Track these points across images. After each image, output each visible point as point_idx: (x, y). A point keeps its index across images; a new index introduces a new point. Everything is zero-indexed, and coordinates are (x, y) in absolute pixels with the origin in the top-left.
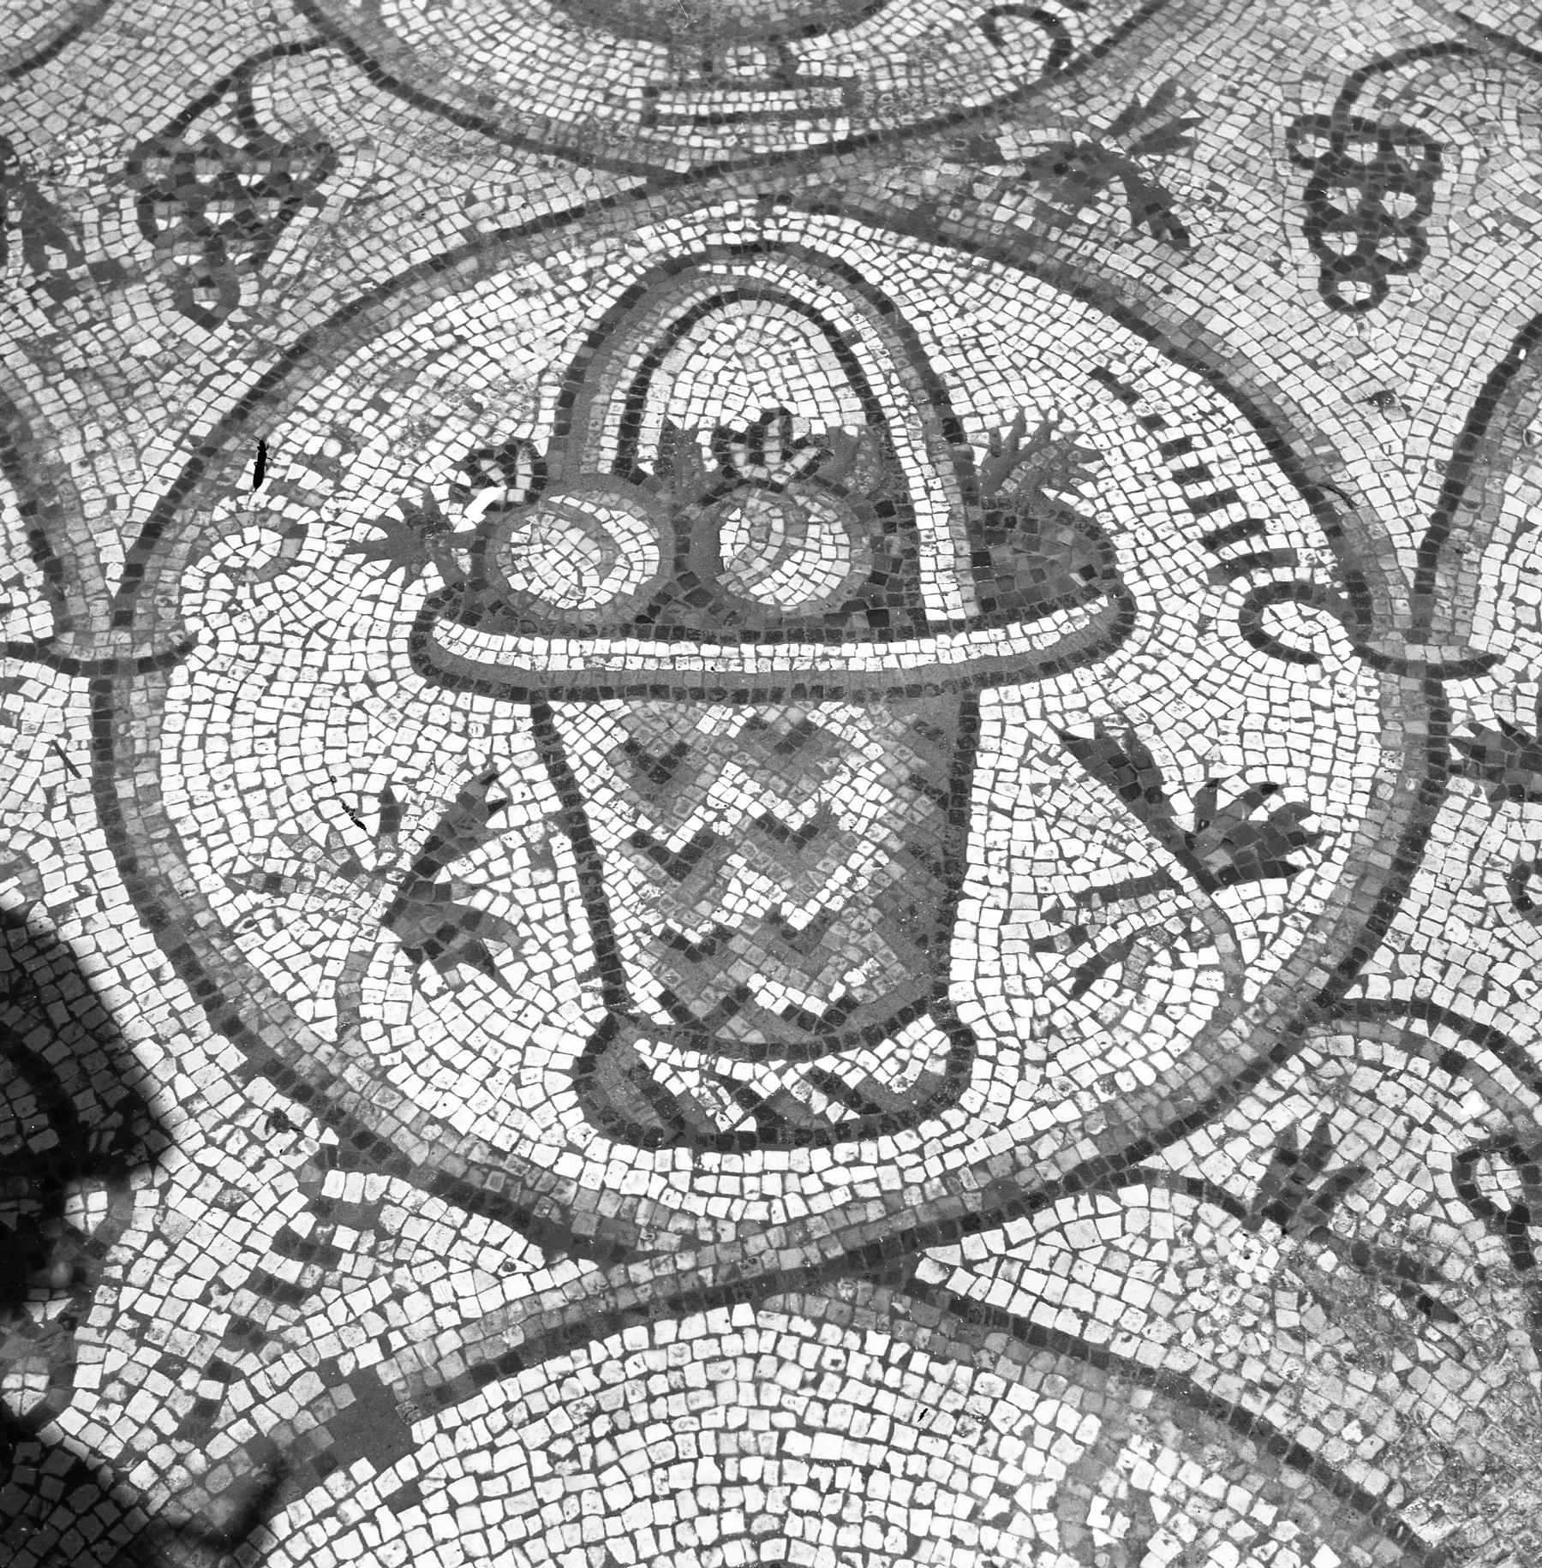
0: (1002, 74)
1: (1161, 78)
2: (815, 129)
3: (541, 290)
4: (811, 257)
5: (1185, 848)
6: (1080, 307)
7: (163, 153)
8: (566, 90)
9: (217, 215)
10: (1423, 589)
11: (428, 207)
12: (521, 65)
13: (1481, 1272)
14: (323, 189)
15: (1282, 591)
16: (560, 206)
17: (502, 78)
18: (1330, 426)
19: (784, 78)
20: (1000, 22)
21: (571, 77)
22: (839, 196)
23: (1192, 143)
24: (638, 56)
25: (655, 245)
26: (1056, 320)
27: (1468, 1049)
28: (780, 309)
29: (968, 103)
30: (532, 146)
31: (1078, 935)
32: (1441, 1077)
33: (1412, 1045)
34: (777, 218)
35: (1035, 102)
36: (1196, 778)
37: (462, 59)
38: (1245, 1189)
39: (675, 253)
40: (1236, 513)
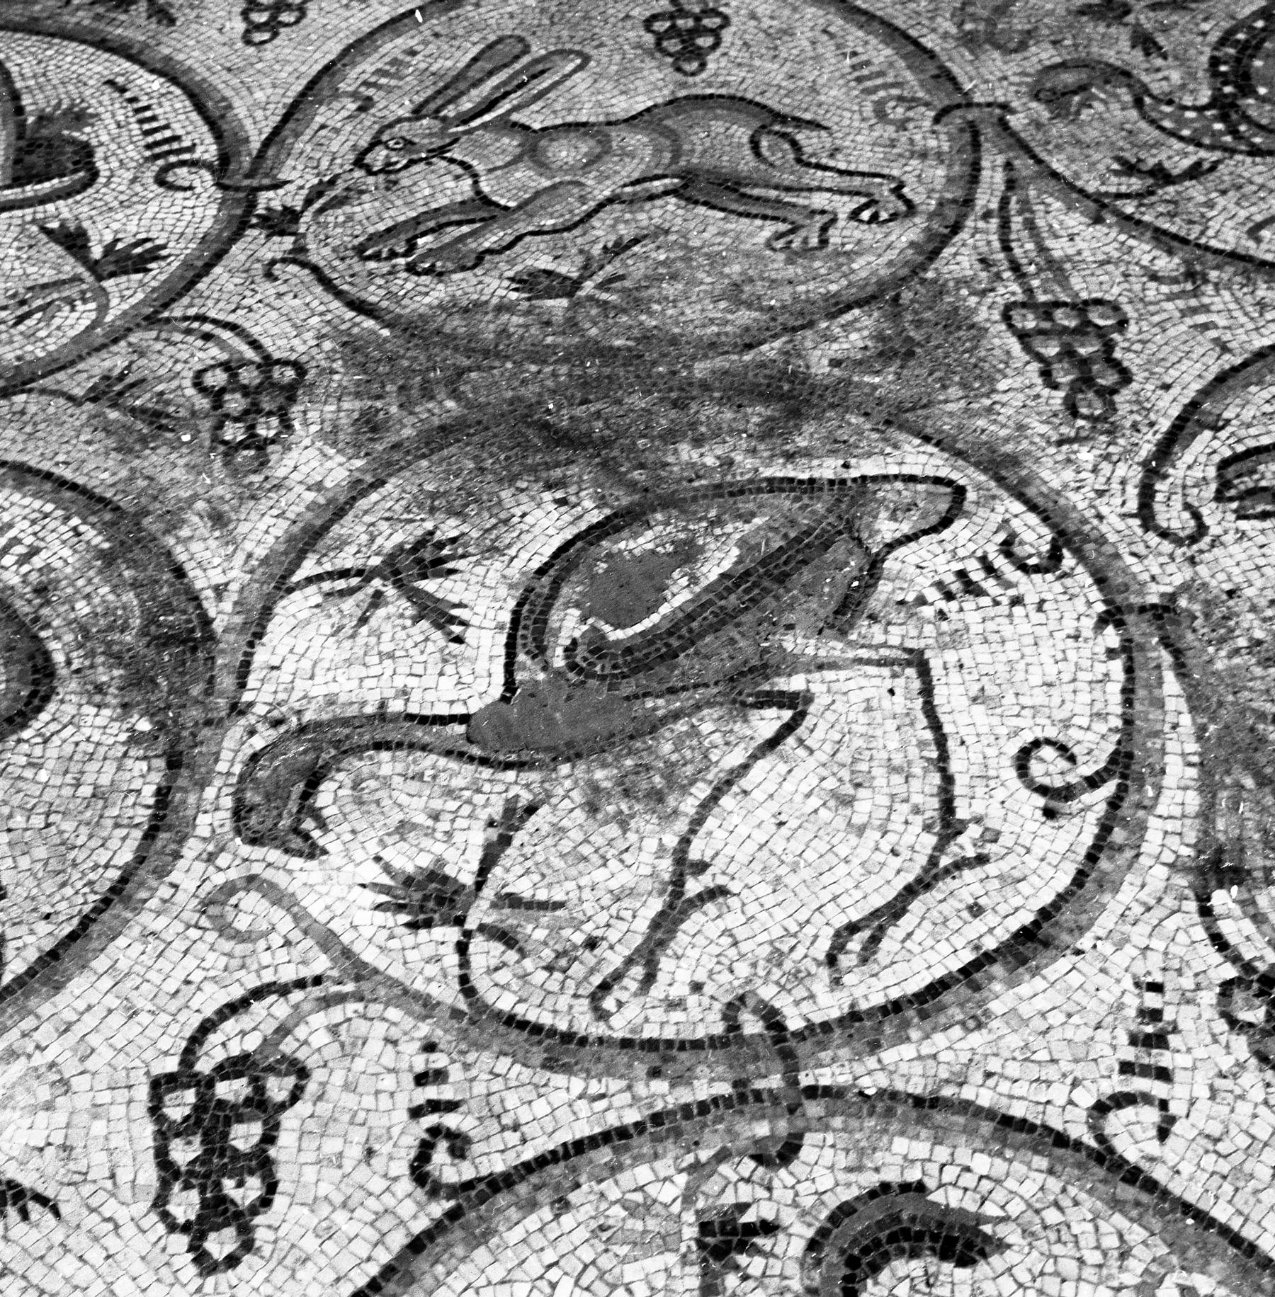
5: (93, 266)
10: (261, 154)
13: (194, 414)
15: (183, 163)
18: (228, 93)
27: (219, 331)
31: (23, 303)
32: (200, 343)
33: (188, 332)
36: (109, 238)
38: (78, 392)
40: (168, 133)
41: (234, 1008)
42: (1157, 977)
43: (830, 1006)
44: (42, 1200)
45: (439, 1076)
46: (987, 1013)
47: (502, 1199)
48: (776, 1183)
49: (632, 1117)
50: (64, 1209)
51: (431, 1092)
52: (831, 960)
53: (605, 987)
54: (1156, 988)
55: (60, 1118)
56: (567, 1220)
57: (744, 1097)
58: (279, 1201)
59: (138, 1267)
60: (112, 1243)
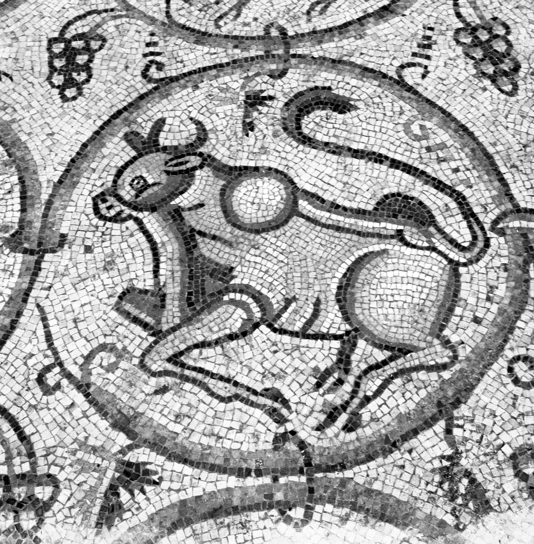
41: (80, 18)
42: (432, 26)
43: (305, 27)
44: (6, 75)
45: (155, 44)
46: (365, 34)
47: (174, 84)
48: (276, 84)
49: (225, 60)
50: (14, 78)
51: (151, 49)
52: (308, 13)
53: (221, 17)
54: (431, 29)
55: (14, 49)
56: (197, 92)
57: (268, 56)
58: (92, 81)
59: (40, 98)
60: (31, 90)
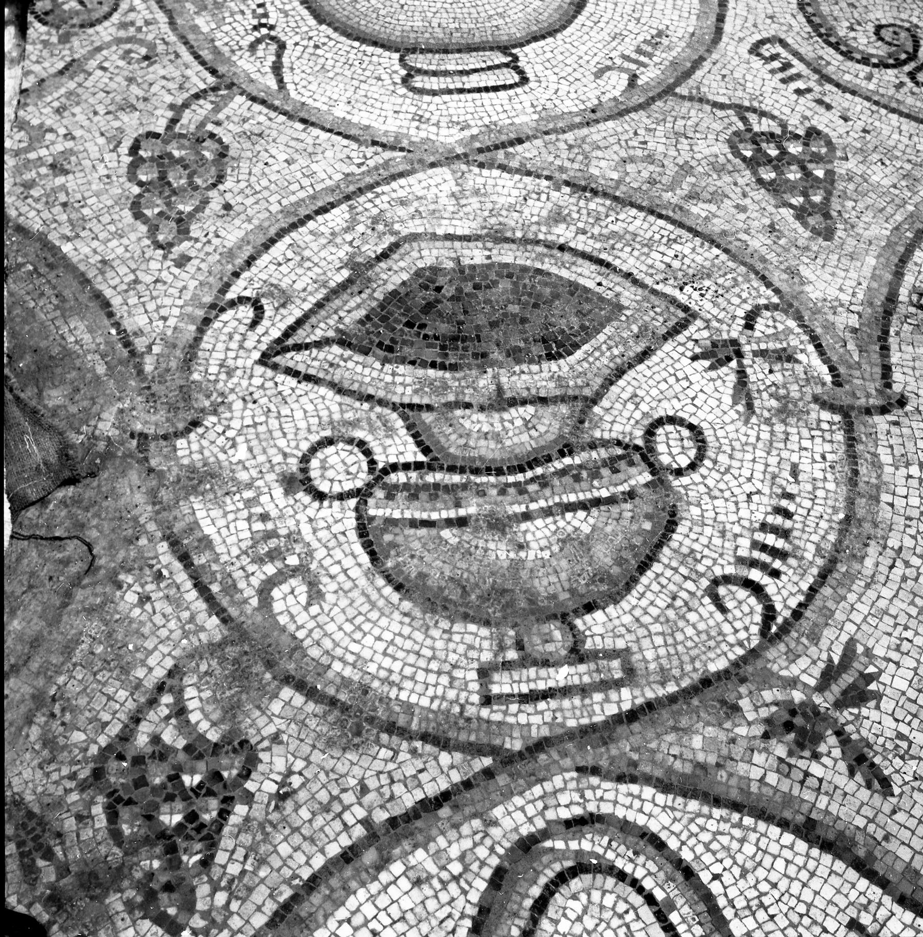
0: (731, 639)
1: (844, 638)
2: (607, 700)
3: (429, 877)
4: (625, 827)
6: (827, 859)
7: (121, 757)
8: (421, 676)
9: (171, 818)
11: (333, 798)
12: (385, 654)
14: (250, 786)
16: (431, 790)
17: (372, 668)
19: (577, 655)
20: (722, 590)
21: (422, 663)
22: (635, 764)
23: (878, 696)
24: (469, 639)
25: (507, 823)
26: (813, 874)
28: (610, 882)
29: (713, 668)
30: (404, 733)
34: (594, 788)
35: (759, 664)
37: (339, 652)
39: (525, 831)
